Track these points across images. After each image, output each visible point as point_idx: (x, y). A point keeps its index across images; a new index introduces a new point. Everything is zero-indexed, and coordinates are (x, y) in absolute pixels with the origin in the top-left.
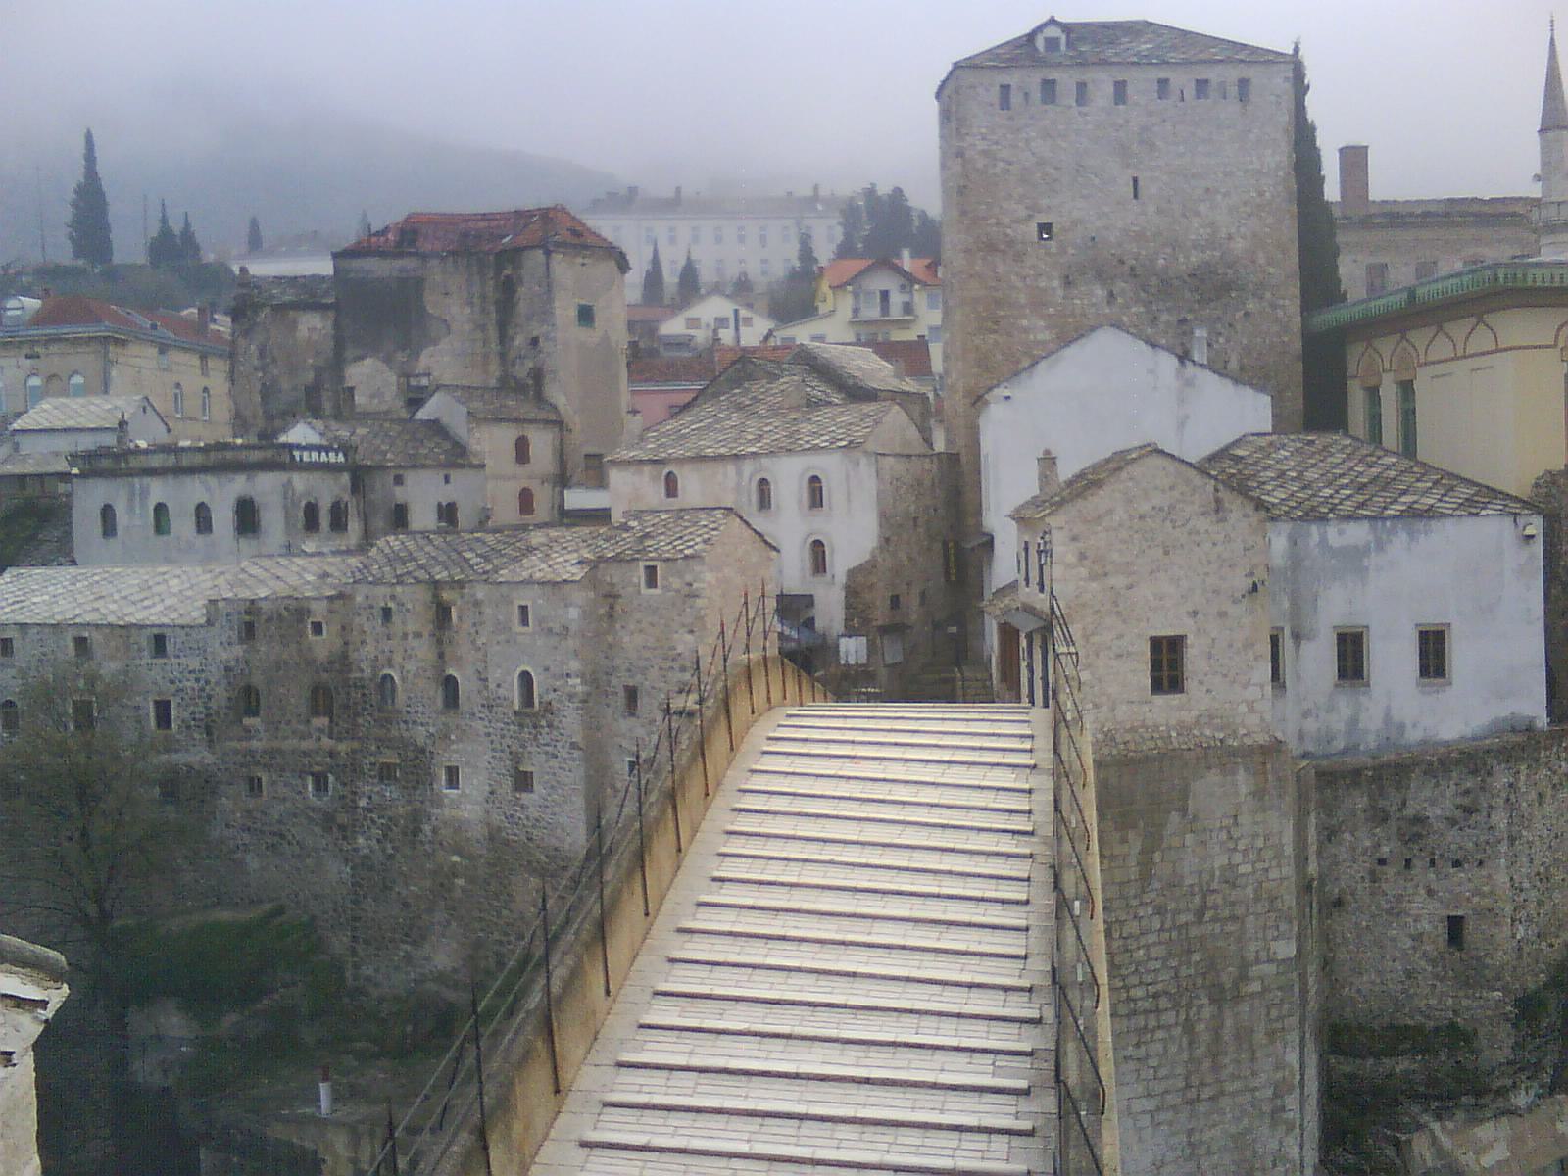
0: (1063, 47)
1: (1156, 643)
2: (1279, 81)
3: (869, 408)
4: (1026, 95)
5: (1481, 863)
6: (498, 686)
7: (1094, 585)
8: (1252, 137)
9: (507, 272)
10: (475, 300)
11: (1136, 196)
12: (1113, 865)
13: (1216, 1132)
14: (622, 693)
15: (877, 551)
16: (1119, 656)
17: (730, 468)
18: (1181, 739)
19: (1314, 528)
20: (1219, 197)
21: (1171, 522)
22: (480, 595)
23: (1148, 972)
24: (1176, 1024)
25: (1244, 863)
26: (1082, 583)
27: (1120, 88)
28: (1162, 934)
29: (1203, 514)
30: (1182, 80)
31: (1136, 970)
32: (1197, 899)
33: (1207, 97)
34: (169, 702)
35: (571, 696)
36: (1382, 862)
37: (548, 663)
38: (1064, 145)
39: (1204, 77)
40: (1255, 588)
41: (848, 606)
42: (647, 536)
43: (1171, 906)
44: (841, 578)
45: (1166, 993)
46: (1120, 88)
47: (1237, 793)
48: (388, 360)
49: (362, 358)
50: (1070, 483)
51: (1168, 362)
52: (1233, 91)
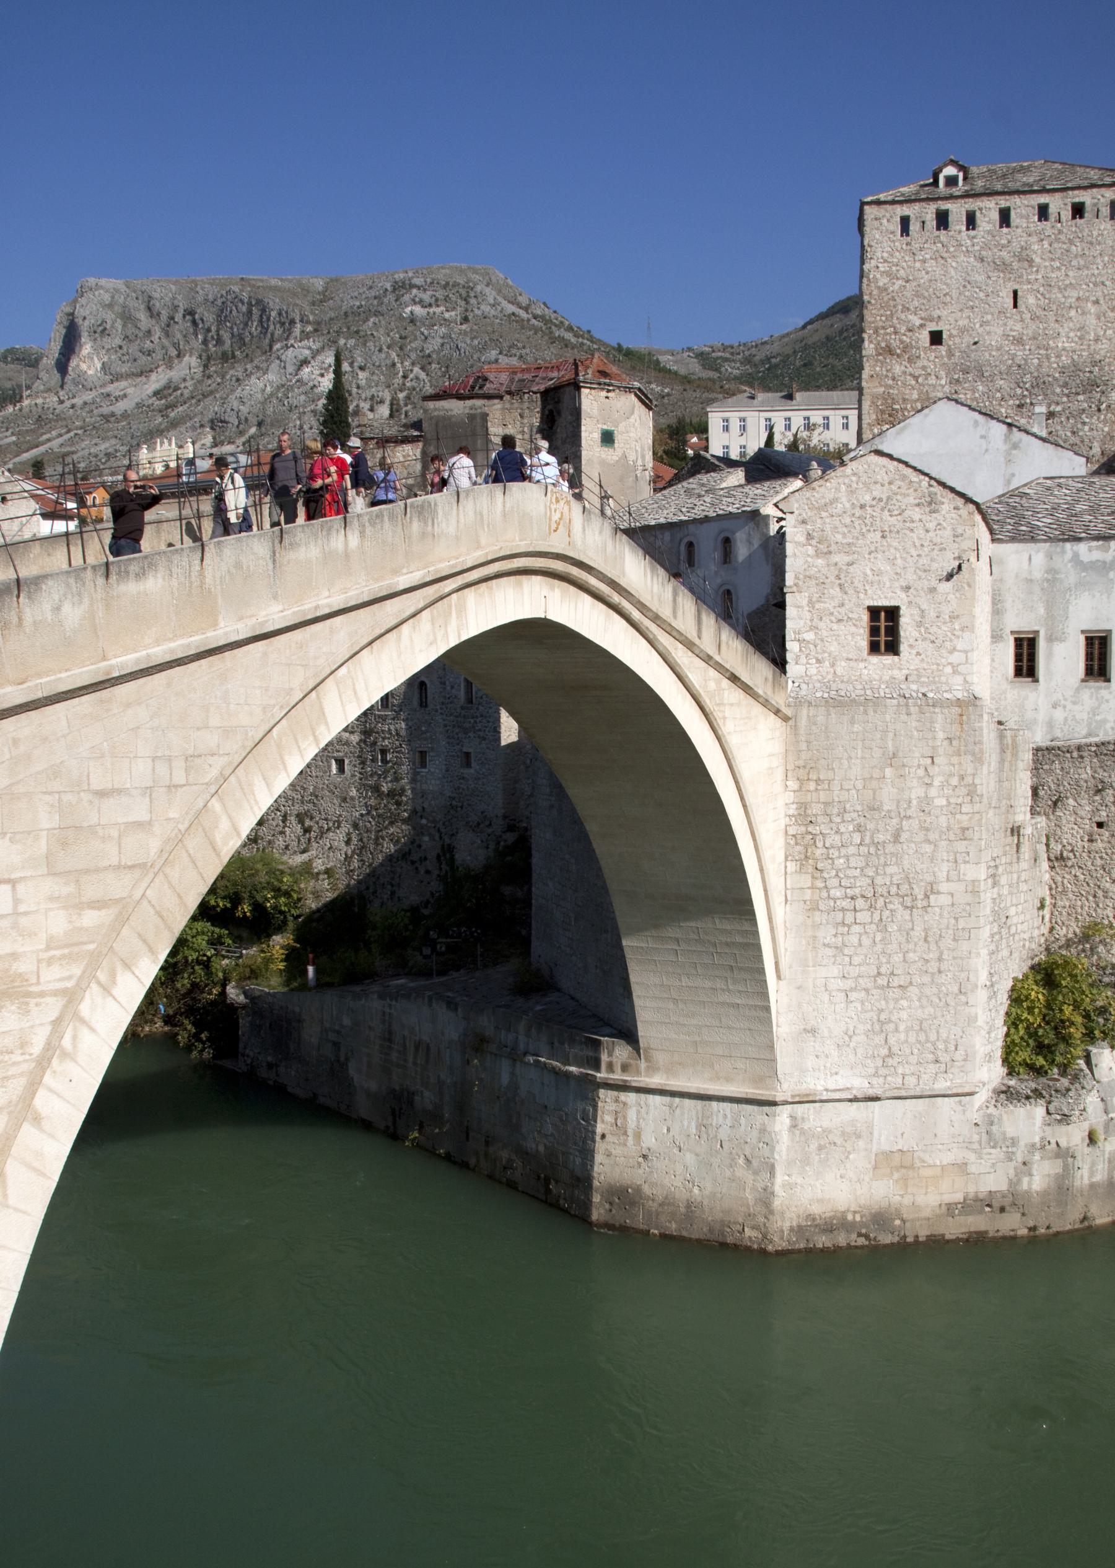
1: (874, 612)
4: (923, 222)
7: (820, 561)
10: (526, 429)
11: (1015, 306)
12: (819, 787)
13: (904, 1015)
15: (770, 597)
16: (840, 621)
18: (887, 691)
19: (1068, 545)
20: (1089, 305)
21: (889, 511)
23: (847, 877)
24: (871, 923)
25: (939, 797)
26: (809, 559)
27: (1005, 217)
28: (861, 848)
29: (918, 505)
30: (1058, 204)
31: (837, 875)
32: (895, 821)
33: (1081, 217)
38: (954, 264)
39: (1077, 200)
40: (960, 567)
43: (871, 826)
45: (863, 896)
46: (1005, 217)
47: (934, 738)
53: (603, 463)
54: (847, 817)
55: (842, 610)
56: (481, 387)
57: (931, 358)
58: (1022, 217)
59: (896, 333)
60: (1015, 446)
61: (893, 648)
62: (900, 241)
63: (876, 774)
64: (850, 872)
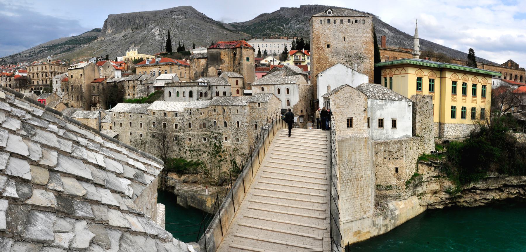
2: (370, 20)
3: (298, 76)
5: (401, 159)
7: (337, 109)
8: (365, 30)
11: (344, 40)
14: (254, 126)
17: (273, 86)
19: (375, 100)
22: (230, 108)
30: (352, 20)
32: (354, 163)
35: (246, 126)
36: (385, 158)
40: (365, 110)
42: (258, 98)
43: (350, 165)
48: (215, 67)
49: (210, 67)
50: (333, 91)
51: (350, 70)
53: (247, 65)
54: (345, 163)
55: (342, 120)
56: (218, 47)
57: (327, 50)
59: (320, 44)
60: (354, 74)
61: (351, 126)
63: (351, 154)
64: (346, 175)
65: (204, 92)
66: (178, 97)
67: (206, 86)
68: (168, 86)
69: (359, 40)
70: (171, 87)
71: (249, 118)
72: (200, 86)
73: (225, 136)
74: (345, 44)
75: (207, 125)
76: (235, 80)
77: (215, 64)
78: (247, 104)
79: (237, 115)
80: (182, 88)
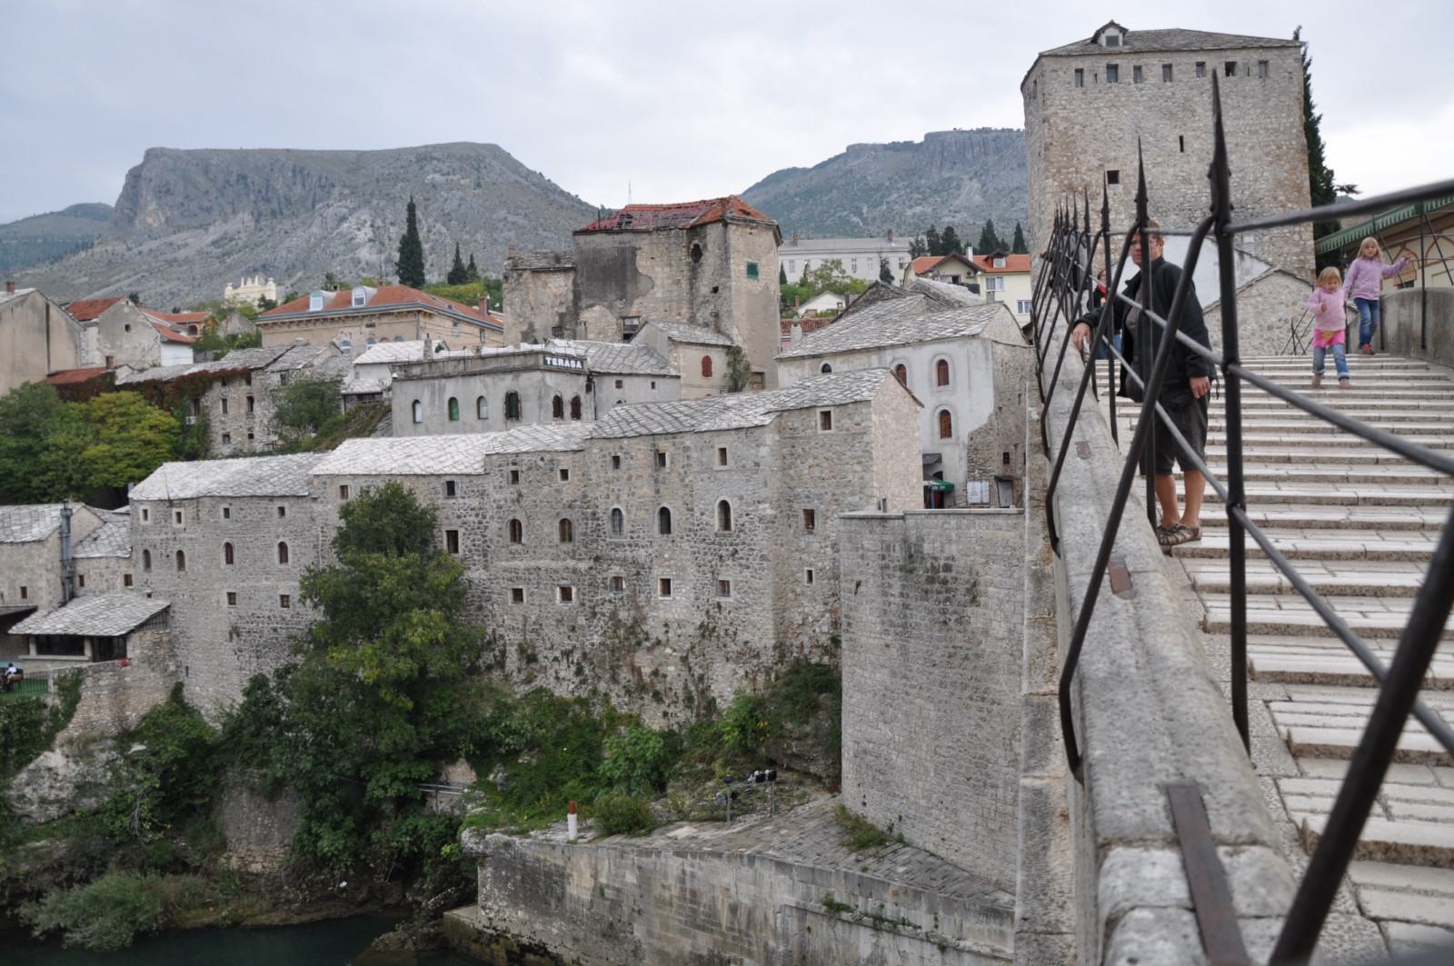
0: (1121, 43)
2: (1290, 61)
6: (702, 514)
8: (1271, 103)
9: (696, 242)
11: (1182, 150)
14: (802, 516)
22: (688, 443)
27: (1168, 68)
34: (456, 532)
37: (742, 493)
41: (970, 461)
44: (964, 438)
48: (610, 307)
49: (591, 306)
52: (1255, 70)
58: (1181, 72)
62: (1077, 92)
65: (567, 398)
66: (455, 423)
67: (578, 373)
68: (410, 378)
69: (1244, 145)
70: (420, 378)
71: (778, 484)
72: (550, 371)
73: (659, 573)
74: (1186, 167)
75: (578, 530)
76: (698, 354)
77: (613, 297)
78: (767, 420)
79: (719, 475)
80: (472, 380)
